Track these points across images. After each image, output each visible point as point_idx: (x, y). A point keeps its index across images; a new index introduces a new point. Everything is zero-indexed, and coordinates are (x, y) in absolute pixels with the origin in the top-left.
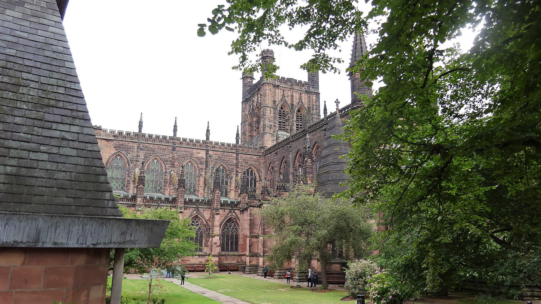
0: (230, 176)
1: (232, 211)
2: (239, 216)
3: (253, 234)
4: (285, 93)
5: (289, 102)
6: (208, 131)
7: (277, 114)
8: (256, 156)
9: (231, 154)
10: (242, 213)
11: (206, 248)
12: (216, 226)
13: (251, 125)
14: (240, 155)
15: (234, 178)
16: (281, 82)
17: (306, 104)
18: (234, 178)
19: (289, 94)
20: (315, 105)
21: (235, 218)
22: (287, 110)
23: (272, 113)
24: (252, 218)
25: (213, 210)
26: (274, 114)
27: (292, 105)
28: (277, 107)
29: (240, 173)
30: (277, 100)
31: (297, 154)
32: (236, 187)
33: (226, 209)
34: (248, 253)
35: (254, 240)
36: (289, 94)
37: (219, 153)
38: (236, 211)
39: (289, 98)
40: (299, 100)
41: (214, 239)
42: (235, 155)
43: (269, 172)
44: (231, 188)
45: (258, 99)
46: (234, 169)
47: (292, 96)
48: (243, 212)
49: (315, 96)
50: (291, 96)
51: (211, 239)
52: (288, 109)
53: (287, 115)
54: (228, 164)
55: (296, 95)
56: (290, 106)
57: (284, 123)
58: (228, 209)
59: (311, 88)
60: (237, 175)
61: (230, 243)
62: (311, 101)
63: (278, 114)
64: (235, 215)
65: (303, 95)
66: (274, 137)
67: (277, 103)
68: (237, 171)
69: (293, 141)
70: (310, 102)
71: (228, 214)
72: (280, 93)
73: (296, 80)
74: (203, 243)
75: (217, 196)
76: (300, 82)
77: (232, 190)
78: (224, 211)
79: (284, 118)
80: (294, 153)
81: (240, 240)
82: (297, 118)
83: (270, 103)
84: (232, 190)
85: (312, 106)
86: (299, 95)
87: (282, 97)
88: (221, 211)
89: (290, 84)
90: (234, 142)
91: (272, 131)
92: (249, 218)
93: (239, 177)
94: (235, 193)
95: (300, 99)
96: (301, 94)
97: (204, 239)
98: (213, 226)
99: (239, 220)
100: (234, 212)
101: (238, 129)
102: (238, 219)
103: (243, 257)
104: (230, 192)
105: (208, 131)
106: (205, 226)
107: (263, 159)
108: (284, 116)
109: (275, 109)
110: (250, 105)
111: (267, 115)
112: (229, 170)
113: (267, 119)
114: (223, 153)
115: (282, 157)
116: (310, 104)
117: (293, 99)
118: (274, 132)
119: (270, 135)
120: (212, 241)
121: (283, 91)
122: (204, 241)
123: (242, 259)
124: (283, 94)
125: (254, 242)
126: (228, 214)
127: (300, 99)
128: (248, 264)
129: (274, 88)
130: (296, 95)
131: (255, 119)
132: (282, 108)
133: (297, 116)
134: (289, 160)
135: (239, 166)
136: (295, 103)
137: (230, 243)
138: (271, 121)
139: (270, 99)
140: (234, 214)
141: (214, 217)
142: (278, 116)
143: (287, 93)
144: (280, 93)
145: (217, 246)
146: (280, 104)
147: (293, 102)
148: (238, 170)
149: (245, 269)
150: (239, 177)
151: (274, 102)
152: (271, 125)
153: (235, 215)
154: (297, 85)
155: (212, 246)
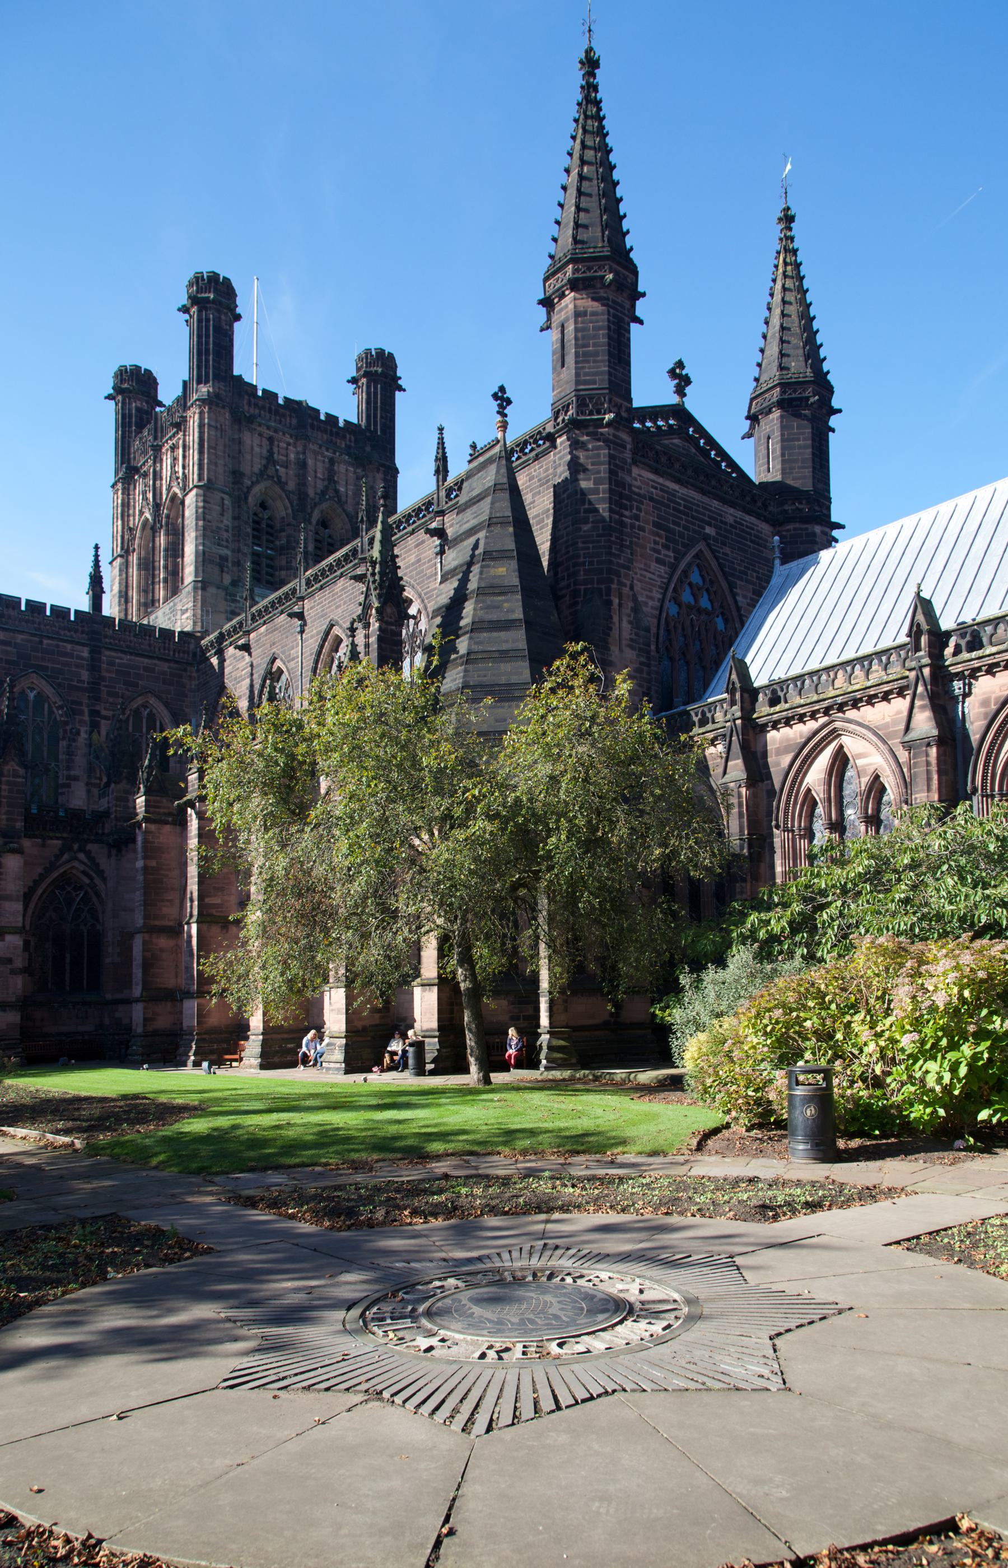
0: (68, 728)
1: (76, 846)
2: (104, 863)
3: (157, 923)
4: (275, 450)
5: (291, 486)
7: (246, 523)
8: (166, 665)
9: (69, 646)
10: (114, 852)
12: (8, 898)
13: (147, 566)
14: (108, 653)
15: (84, 735)
16: (263, 408)
17: (350, 501)
18: (84, 735)
19: (292, 456)
21: (87, 869)
22: (281, 509)
23: (229, 514)
26: (234, 518)
27: (303, 496)
28: (246, 498)
29: (106, 718)
30: (246, 469)
31: (324, 640)
32: (90, 770)
33: (51, 838)
34: (137, 991)
35: (163, 942)
36: (292, 456)
37: (20, 638)
38: (89, 847)
40: (326, 483)
42: (85, 653)
44: (72, 773)
45: (173, 466)
46: (81, 704)
47: (303, 465)
48: (119, 850)
49: (379, 476)
52: (286, 509)
53: (282, 530)
54: (59, 685)
55: (317, 466)
56: (295, 498)
57: (271, 558)
58: (58, 838)
59: (368, 449)
60: (95, 726)
64: (85, 860)
65: (342, 468)
66: (234, 601)
67: (248, 482)
68: (94, 713)
69: (311, 595)
71: (58, 857)
72: (257, 449)
73: (317, 412)
76: (332, 419)
77: (76, 779)
78: (44, 846)
79: (272, 542)
80: (312, 637)
81: (110, 950)
82: (316, 548)
83: (221, 477)
84: (76, 779)
86: (327, 465)
87: (264, 462)
88: (27, 843)
89: (294, 421)
90: (82, 603)
91: (227, 579)
93: (103, 733)
94: (89, 791)
95: (331, 478)
96: (332, 461)
99: (104, 880)
100: (80, 850)
101: (97, 556)
102: (101, 873)
104: (68, 786)
107: (195, 674)
108: (271, 535)
109: (240, 499)
110: (144, 493)
112: (61, 707)
114: (37, 639)
115: (267, 659)
118: (235, 583)
119: (222, 593)
121: (271, 440)
123: (117, 1015)
124: (271, 452)
125: (162, 950)
126: (58, 857)
127: (331, 478)
128: (140, 1030)
129: (237, 427)
130: (317, 466)
132: (263, 505)
133: (316, 540)
134: (292, 665)
135: (104, 695)
136: (311, 492)
138: (224, 543)
139: (221, 462)
140: (82, 856)
142: (249, 530)
144: (257, 449)
146: (257, 489)
147: (304, 484)
148: (98, 708)
149: (127, 1048)
150: (103, 733)
151: (237, 475)
152: (224, 559)
153: (85, 860)
154: (319, 429)
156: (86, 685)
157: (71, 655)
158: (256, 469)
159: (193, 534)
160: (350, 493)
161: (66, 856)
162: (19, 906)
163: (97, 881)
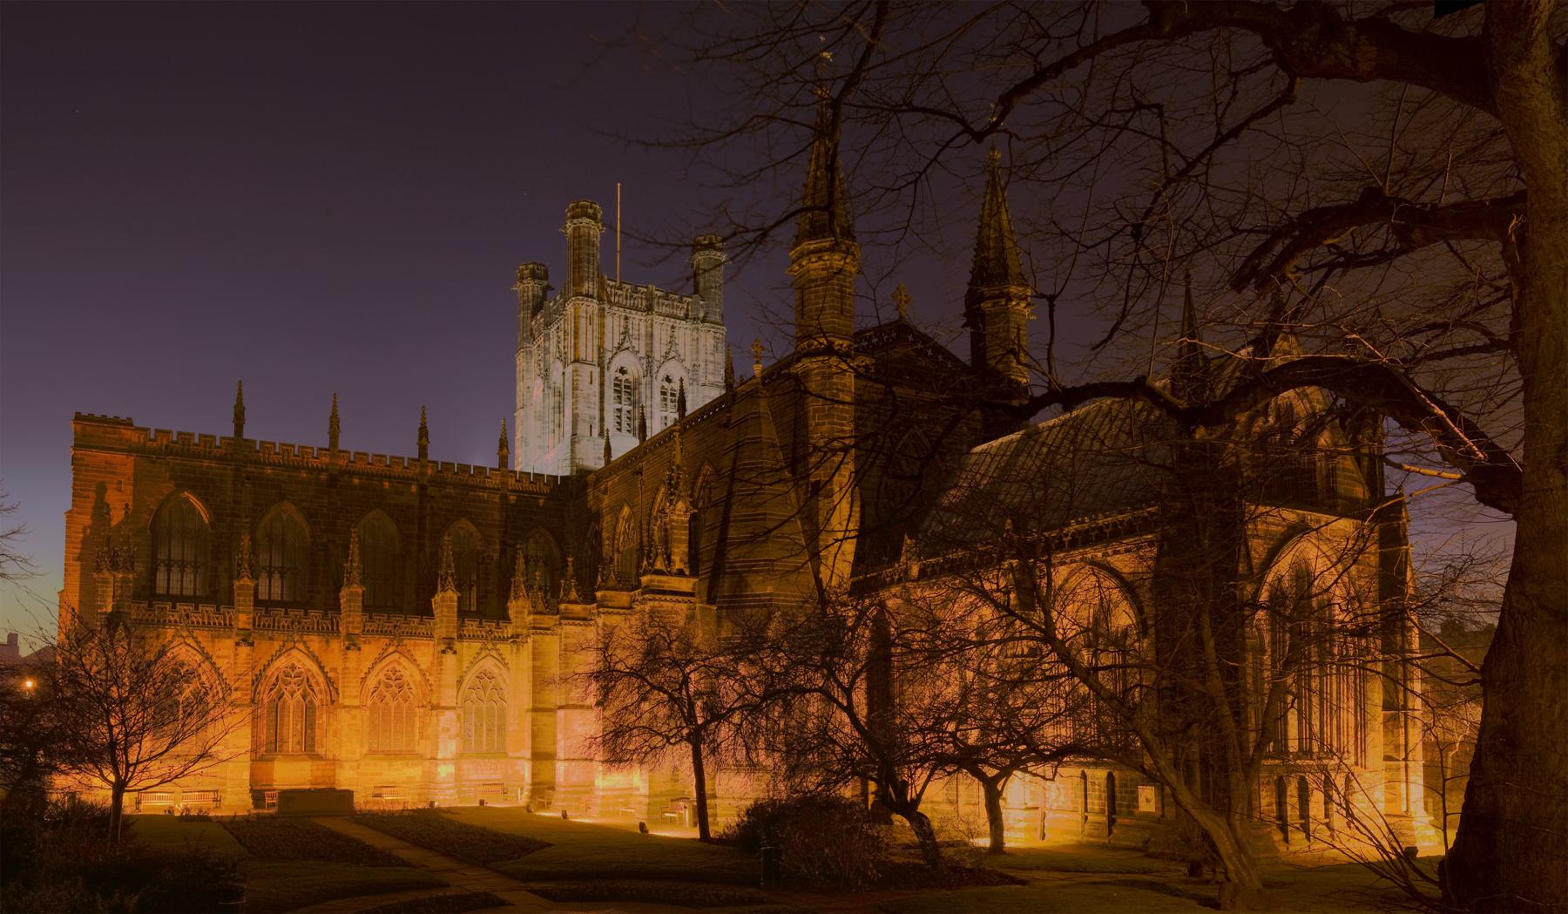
4: (630, 327)
5: (642, 353)
6: (423, 433)
11: (422, 742)
17: (688, 359)
20: (711, 362)
24: (538, 664)
25: (439, 644)
35: (544, 718)
38: (498, 646)
39: (642, 343)
41: (442, 718)
43: (587, 543)
50: (646, 335)
51: (434, 719)
61: (485, 728)
62: (702, 351)
63: (613, 387)
65: (679, 333)
70: (697, 352)
74: (417, 731)
75: (447, 606)
85: (703, 365)
86: (669, 332)
92: (530, 664)
97: (417, 719)
98: (440, 686)
103: (519, 762)
104: (486, 597)
105: (423, 433)
106: (421, 685)
111: (581, 387)
113: (580, 399)
116: (697, 360)
117: (652, 344)
120: (438, 725)
122: (417, 724)
123: (517, 768)
125: (544, 725)
126: (478, 653)
131: (552, 401)
137: (485, 728)
141: (441, 664)
143: (636, 327)
144: (617, 329)
145: (450, 738)
147: (652, 351)
155: (437, 737)
156: (497, 523)
157: (487, 502)
158: (616, 345)
159: (571, 401)
160: (688, 353)
161: (483, 655)
162: (455, 692)
163: (504, 670)
